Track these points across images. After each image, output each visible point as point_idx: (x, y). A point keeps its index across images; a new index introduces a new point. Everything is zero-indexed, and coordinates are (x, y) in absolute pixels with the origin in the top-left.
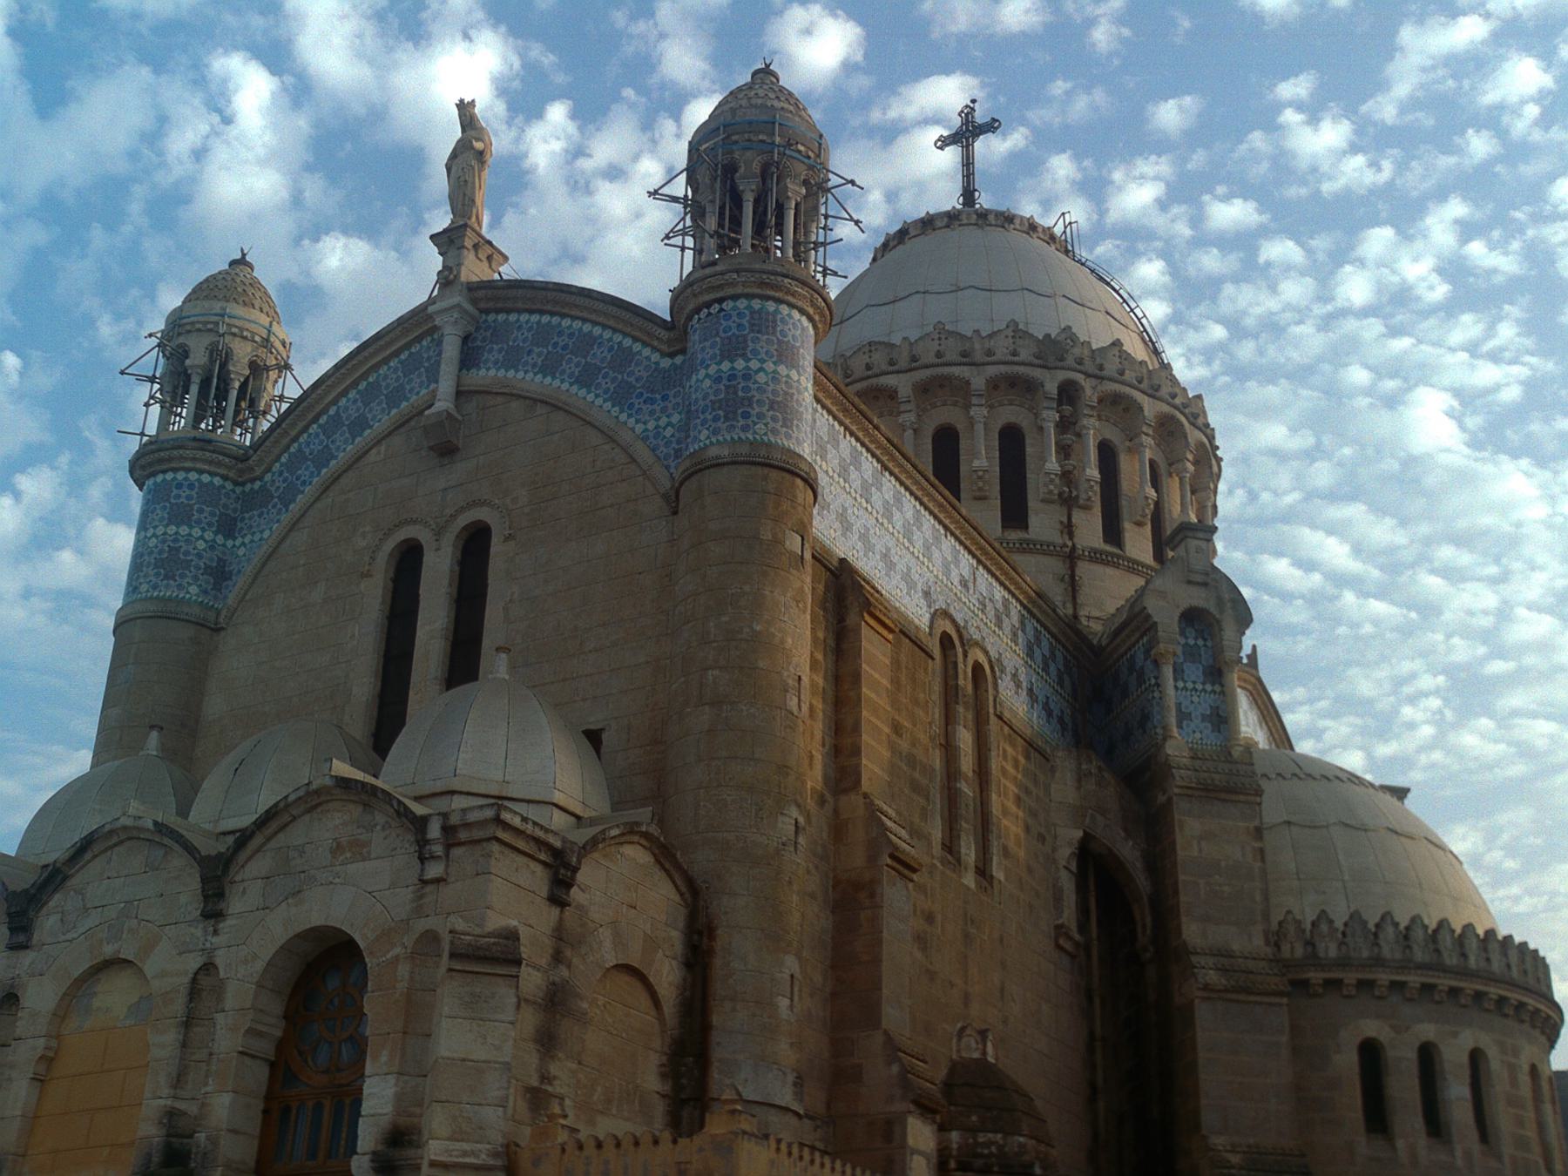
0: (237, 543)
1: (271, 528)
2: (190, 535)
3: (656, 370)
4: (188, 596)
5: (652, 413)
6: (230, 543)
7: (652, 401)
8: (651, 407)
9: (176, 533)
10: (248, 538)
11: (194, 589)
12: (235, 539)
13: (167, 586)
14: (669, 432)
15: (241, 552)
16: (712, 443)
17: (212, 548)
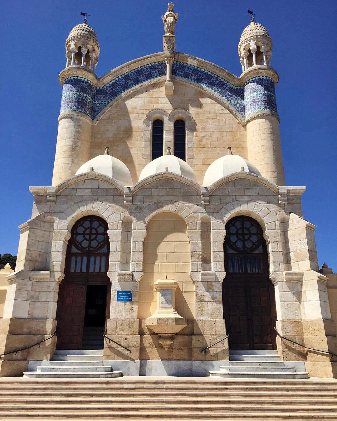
0: (96, 102)
1: (108, 101)
2: (86, 96)
3: (232, 89)
4: (87, 114)
5: (232, 99)
6: (94, 102)
7: (232, 96)
8: (232, 98)
9: (83, 95)
10: (100, 102)
11: (88, 112)
12: (95, 101)
13: (82, 109)
14: (238, 105)
15: (98, 105)
16: (265, 110)
17: (91, 102)
